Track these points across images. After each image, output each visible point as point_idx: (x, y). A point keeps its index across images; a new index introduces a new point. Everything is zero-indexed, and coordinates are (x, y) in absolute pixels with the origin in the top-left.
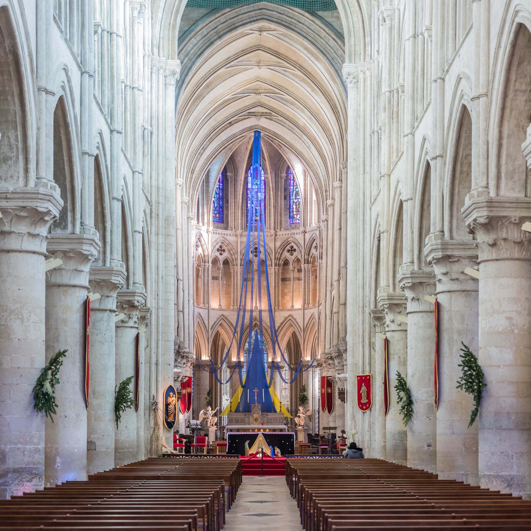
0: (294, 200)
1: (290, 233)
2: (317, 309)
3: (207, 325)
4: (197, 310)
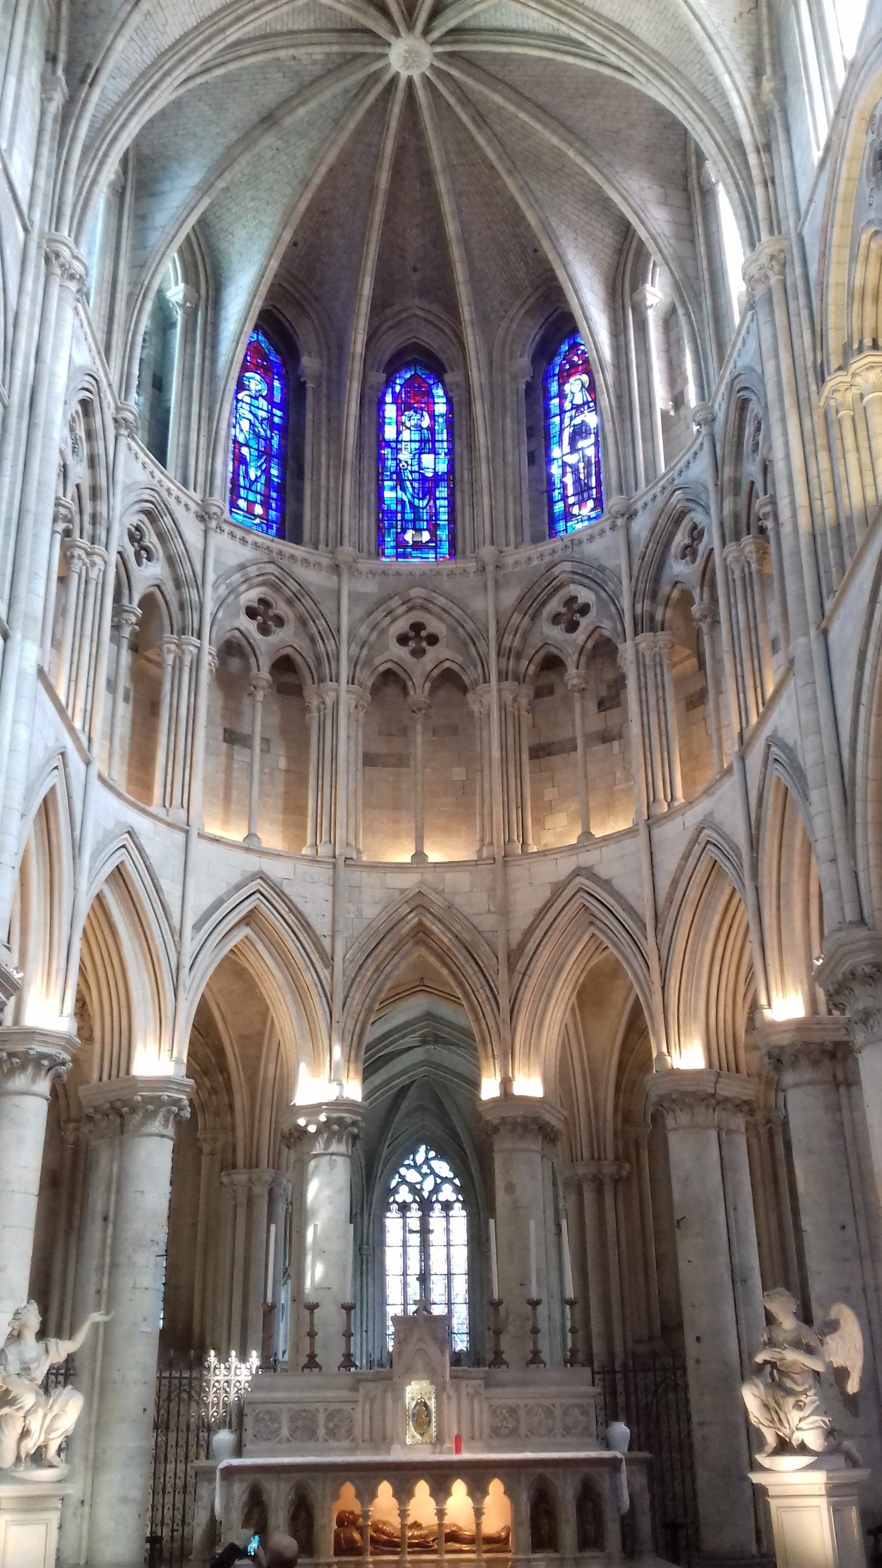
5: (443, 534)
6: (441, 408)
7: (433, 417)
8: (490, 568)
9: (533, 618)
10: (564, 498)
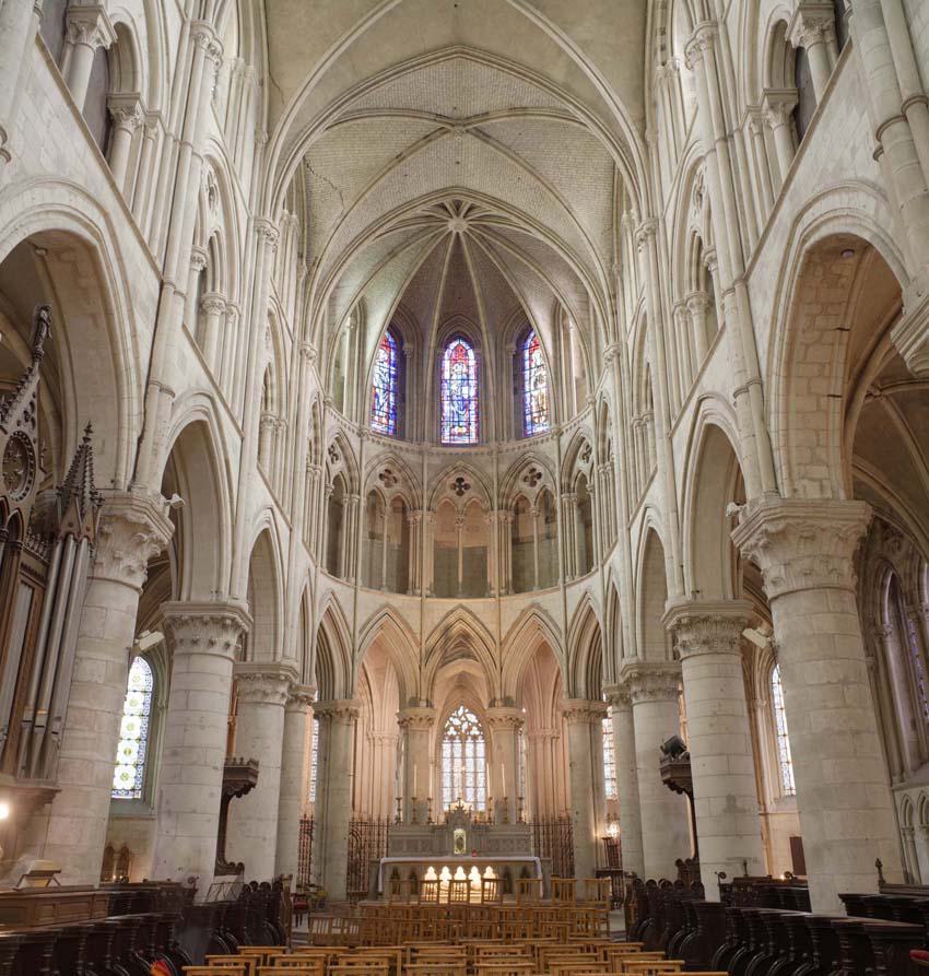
0: (533, 393)
1: (527, 443)
2: (599, 573)
3: (350, 620)
4: (325, 582)
5: (473, 428)
6: (472, 362)
7: (468, 367)
8: (495, 453)
9: (515, 479)
10: (531, 413)
